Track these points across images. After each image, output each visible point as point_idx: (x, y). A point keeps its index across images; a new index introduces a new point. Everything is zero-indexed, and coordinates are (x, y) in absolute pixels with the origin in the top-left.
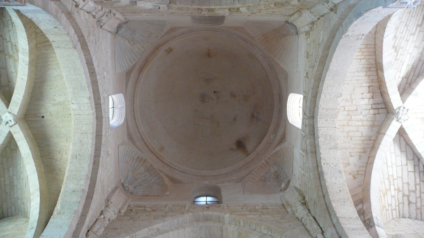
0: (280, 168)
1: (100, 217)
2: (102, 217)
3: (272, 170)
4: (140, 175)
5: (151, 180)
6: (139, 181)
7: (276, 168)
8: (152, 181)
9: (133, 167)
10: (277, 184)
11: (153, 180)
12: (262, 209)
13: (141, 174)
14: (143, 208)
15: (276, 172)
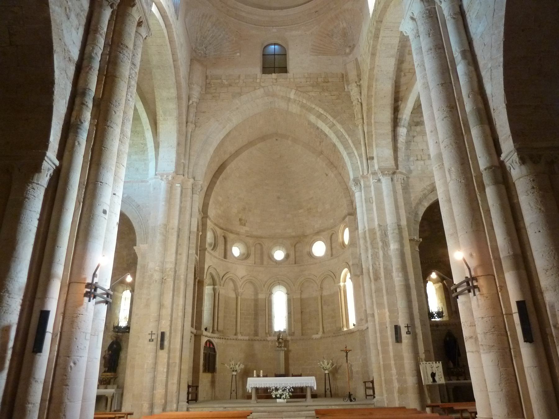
0: (349, 27)
1: (189, 104)
2: (191, 102)
3: (341, 26)
4: (208, 32)
5: (220, 35)
6: (208, 39)
7: (345, 25)
8: (220, 37)
9: (200, 26)
10: (343, 43)
11: (222, 35)
12: (323, 82)
13: (209, 31)
14: (219, 81)
15: (344, 28)
